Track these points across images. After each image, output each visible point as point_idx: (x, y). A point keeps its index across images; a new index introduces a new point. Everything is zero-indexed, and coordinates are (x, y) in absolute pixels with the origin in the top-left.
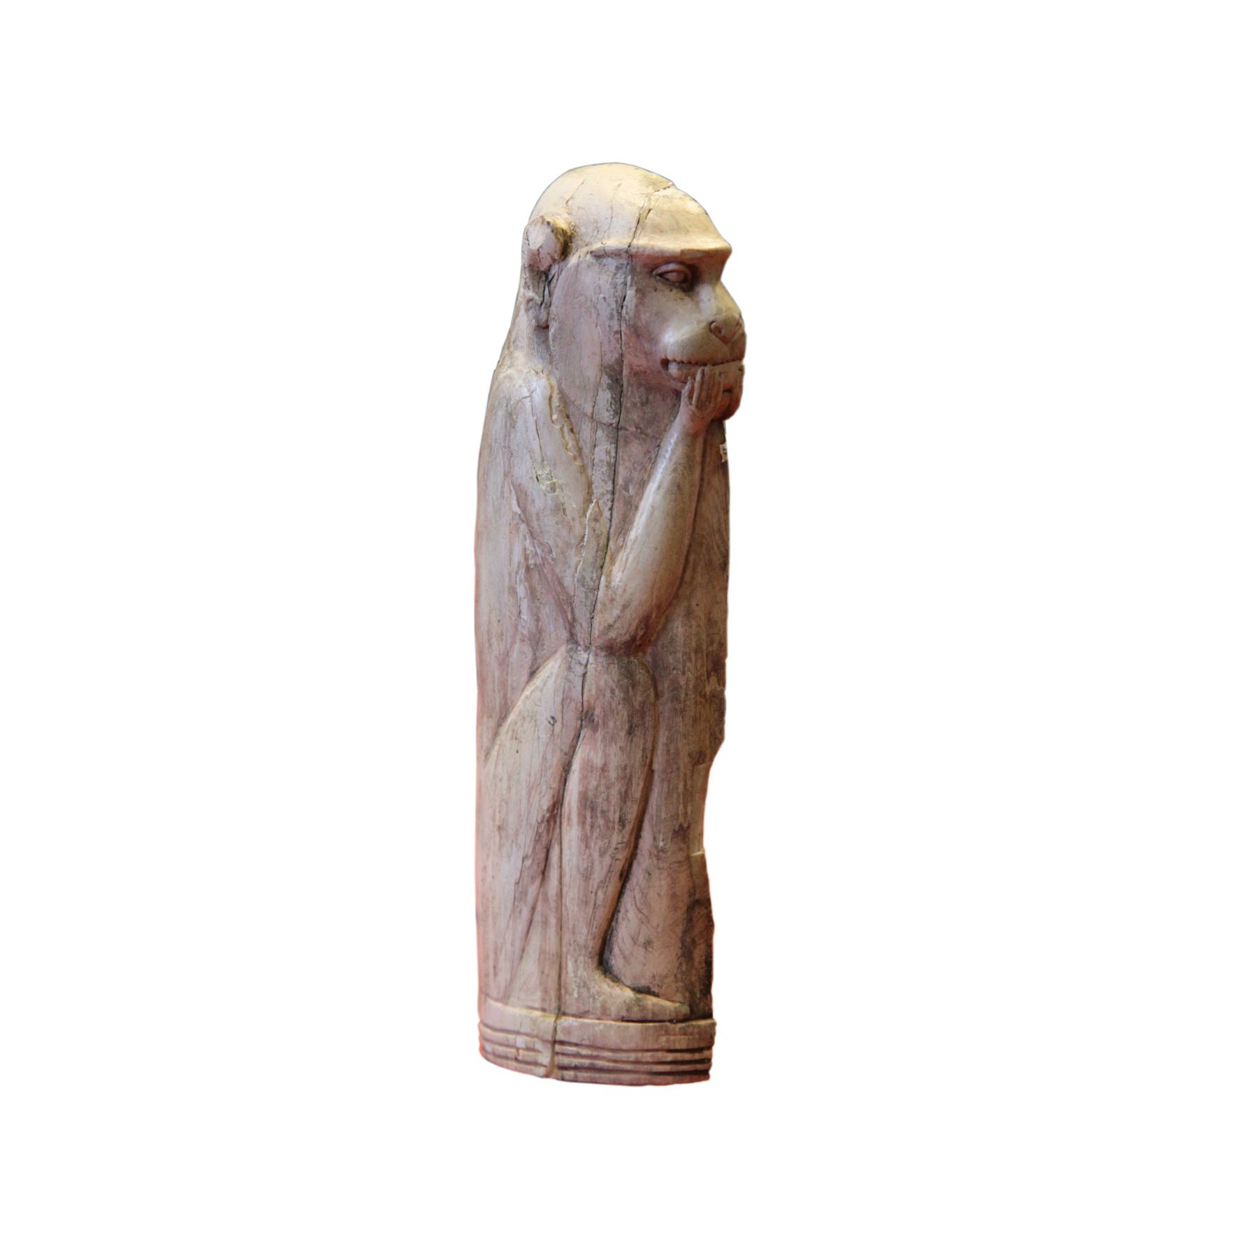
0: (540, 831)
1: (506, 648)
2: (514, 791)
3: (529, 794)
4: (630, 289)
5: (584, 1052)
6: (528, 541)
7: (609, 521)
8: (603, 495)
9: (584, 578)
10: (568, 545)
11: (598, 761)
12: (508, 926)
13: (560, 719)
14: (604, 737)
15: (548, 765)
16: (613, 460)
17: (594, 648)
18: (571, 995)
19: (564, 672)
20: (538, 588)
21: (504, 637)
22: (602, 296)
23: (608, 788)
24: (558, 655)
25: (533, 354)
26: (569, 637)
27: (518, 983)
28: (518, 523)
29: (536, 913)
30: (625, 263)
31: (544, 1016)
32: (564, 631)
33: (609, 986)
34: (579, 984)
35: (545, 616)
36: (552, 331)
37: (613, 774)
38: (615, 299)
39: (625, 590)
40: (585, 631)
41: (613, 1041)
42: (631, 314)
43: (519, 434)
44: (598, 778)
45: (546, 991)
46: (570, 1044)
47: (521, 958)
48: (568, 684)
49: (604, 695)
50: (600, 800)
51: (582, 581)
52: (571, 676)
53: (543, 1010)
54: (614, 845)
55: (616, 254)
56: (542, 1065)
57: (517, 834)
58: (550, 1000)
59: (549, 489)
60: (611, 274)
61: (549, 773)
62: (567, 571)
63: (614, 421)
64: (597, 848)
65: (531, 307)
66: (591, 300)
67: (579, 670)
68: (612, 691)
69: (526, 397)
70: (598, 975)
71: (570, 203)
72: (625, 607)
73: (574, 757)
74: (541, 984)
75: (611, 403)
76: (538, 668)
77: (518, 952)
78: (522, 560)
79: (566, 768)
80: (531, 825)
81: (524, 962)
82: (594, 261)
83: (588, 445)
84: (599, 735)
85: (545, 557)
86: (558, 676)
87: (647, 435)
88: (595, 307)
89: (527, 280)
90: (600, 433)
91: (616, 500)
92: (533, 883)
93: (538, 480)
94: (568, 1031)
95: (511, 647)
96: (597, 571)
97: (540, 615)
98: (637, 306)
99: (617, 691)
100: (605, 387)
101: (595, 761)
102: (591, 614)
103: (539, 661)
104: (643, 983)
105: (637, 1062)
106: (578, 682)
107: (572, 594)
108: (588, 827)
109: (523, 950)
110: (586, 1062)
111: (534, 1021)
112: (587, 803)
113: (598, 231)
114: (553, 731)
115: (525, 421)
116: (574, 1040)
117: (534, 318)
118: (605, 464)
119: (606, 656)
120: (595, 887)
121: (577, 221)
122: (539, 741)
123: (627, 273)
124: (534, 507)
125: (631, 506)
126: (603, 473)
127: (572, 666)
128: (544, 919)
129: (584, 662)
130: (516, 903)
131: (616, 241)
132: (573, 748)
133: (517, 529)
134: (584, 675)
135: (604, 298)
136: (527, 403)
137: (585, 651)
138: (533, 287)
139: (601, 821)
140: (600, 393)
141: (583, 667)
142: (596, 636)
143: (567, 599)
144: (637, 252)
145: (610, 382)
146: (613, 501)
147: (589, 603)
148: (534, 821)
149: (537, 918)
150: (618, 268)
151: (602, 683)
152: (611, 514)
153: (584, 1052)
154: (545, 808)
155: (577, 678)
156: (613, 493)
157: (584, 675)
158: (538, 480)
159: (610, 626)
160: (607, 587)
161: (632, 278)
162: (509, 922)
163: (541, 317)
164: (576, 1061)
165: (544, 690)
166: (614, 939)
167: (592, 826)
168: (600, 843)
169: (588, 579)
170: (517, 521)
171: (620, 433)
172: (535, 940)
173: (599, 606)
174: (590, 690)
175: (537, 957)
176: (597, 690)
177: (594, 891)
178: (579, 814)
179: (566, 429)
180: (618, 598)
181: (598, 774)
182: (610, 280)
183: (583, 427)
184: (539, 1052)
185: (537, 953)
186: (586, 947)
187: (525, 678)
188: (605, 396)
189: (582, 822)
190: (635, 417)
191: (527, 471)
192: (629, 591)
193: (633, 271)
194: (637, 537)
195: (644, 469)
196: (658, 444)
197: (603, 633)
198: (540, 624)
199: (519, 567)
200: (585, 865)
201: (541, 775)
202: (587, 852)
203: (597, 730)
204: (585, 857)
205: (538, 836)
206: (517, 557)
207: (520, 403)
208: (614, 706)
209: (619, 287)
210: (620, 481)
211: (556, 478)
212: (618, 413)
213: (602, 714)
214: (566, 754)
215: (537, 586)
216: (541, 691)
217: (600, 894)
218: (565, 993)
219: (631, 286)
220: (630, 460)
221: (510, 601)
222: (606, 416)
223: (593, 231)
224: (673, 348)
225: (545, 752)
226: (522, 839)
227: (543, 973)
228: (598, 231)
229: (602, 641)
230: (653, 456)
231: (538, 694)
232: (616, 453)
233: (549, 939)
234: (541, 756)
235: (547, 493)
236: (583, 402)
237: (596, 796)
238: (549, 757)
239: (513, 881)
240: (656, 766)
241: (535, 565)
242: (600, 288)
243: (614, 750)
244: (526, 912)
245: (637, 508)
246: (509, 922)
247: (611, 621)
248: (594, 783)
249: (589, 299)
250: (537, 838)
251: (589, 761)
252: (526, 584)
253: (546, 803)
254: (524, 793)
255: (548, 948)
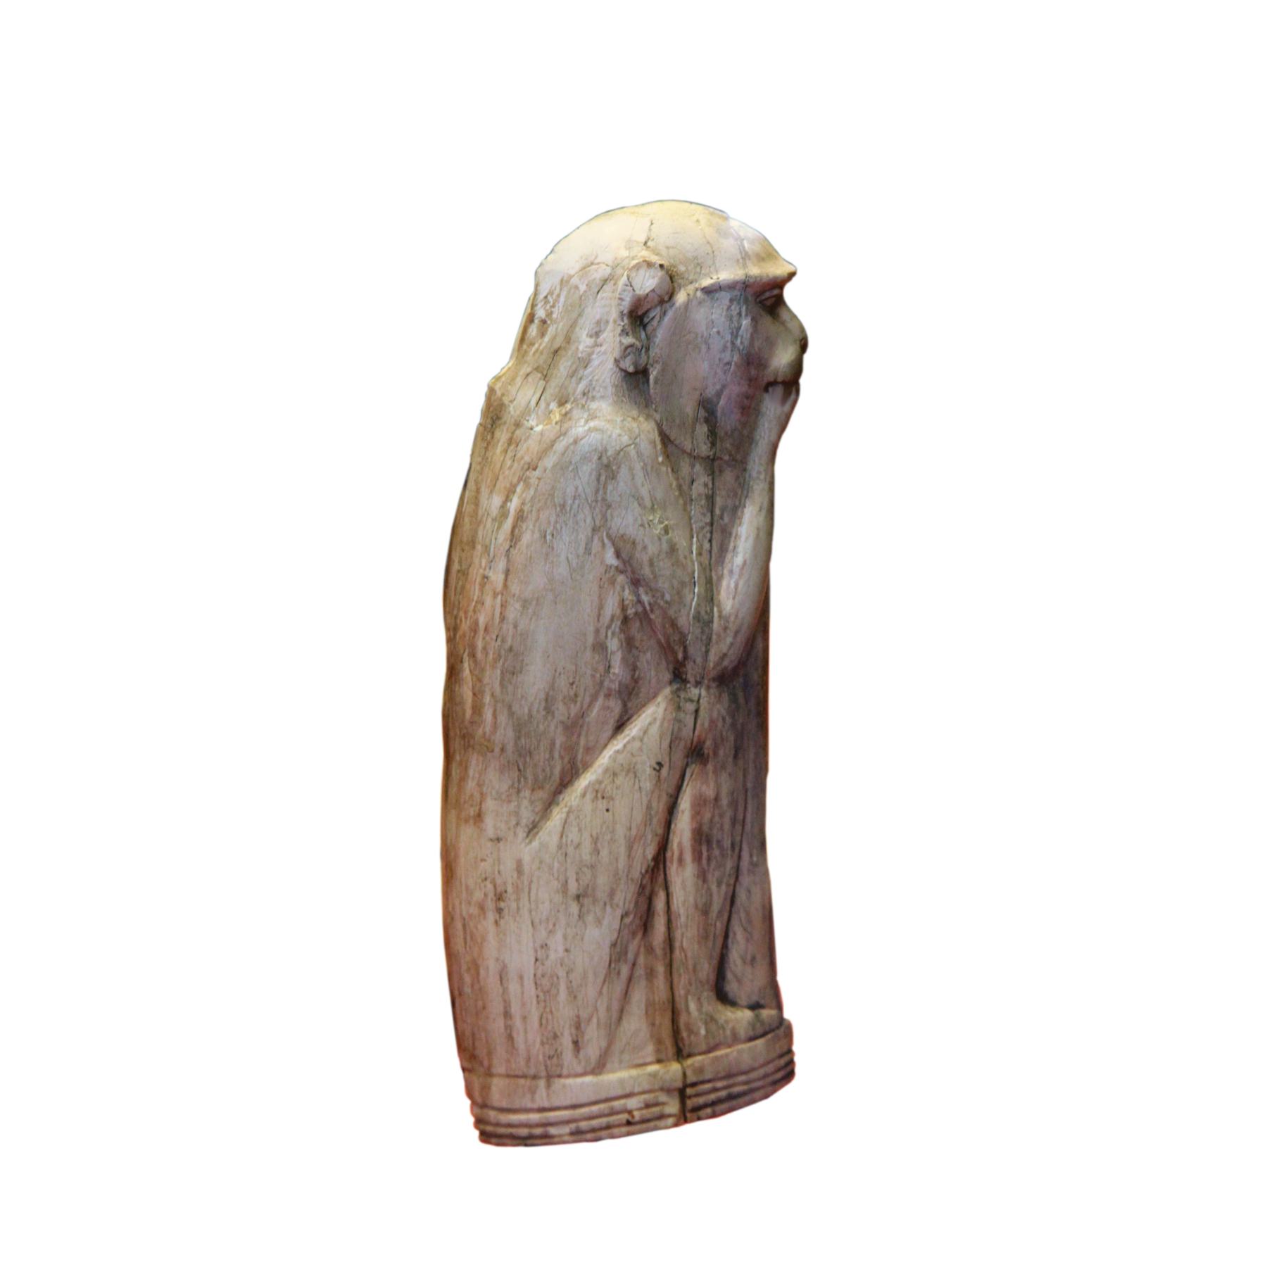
0: (644, 882)
1: (582, 708)
2: (604, 853)
3: (630, 848)
4: (745, 319)
5: (719, 1084)
6: (627, 591)
7: (708, 553)
8: (702, 528)
9: (699, 613)
10: (683, 584)
11: (710, 792)
12: (600, 993)
13: (668, 764)
14: (715, 767)
15: (652, 813)
16: (710, 492)
17: (706, 681)
18: (697, 1034)
19: (672, 713)
20: (638, 636)
21: (579, 699)
22: (715, 330)
23: (721, 816)
24: (660, 699)
25: (622, 401)
26: (673, 677)
27: (617, 1046)
28: (613, 576)
29: (637, 967)
30: (739, 294)
31: (666, 1066)
32: (667, 672)
33: (732, 1012)
34: (706, 1020)
35: (645, 664)
36: (653, 374)
37: (725, 802)
38: (730, 331)
39: (737, 616)
40: (698, 665)
41: (747, 1061)
42: (746, 343)
43: (621, 484)
44: (712, 810)
45: (659, 1042)
46: (703, 1082)
47: (620, 1019)
48: (677, 725)
49: (716, 726)
50: (715, 831)
51: (697, 617)
52: (682, 715)
53: (659, 1061)
54: (727, 873)
55: (731, 286)
56: (670, 1116)
57: (612, 894)
58: (666, 1049)
59: (663, 532)
60: (725, 308)
61: (655, 821)
62: (682, 610)
63: (711, 453)
64: (715, 879)
65: (629, 354)
66: (702, 337)
67: (691, 707)
68: (724, 719)
69: (630, 445)
70: (720, 1007)
71: (649, 244)
72: (737, 633)
73: (681, 796)
74: (652, 1036)
75: (708, 436)
76: (629, 719)
77: (615, 1015)
78: (618, 612)
79: (672, 809)
80: (632, 880)
81: (625, 1022)
82: (706, 297)
83: (687, 482)
84: (710, 767)
85: (656, 602)
86: (664, 719)
87: (736, 461)
88: (706, 343)
89: (626, 327)
90: (698, 468)
91: (714, 530)
92: (633, 938)
93: (650, 526)
94: (700, 1070)
95: (589, 706)
96: (709, 603)
97: (638, 664)
98: (752, 335)
99: (727, 718)
100: (702, 420)
101: (707, 793)
102: (706, 647)
103: (630, 712)
104: (755, 998)
105: (766, 1076)
106: (689, 720)
107: (687, 632)
108: (704, 861)
109: (622, 1011)
110: (723, 1094)
111: (654, 1075)
112: (701, 837)
113: (701, 267)
114: (659, 777)
115: (631, 469)
116: (708, 1076)
117: (633, 363)
118: (704, 497)
119: (718, 686)
120: (714, 918)
121: (672, 261)
122: (641, 792)
123: (742, 303)
124: (647, 553)
125: (727, 533)
126: (702, 506)
127: (681, 704)
128: (649, 971)
129: (696, 699)
130: (613, 965)
131: (727, 274)
132: (679, 788)
133: (612, 582)
134: (697, 711)
135: (718, 333)
136: (632, 449)
137: (696, 686)
138: (633, 333)
139: (716, 852)
140: (698, 426)
141: (695, 703)
142: (711, 669)
143: (680, 639)
144: (754, 283)
145: (707, 415)
146: (711, 533)
147: (704, 637)
148: (636, 874)
149: (640, 971)
150: (731, 301)
151: (715, 714)
152: (711, 546)
153: (719, 1084)
154: (650, 857)
155: (688, 716)
156: (712, 524)
157: (697, 711)
158: (650, 526)
159: (725, 655)
160: (720, 617)
161: (747, 308)
162: (602, 988)
163: (641, 362)
164: (713, 1097)
165: (645, 739)
166: (727, 965)
167: (709, 859)
168: (717, 874)
169: (703, 613)
170: (611, 574)
171: (716, 463)
172: (639, 997)
173: (714, 637)
174: (703, 725)
175: (644, 1012)
176: (710, 723)
177: (713, 923)
178: (694, 850)
179: (670, 470)
180: (731, 625)
181: (712, 805)
182: (724, 313)
183: (682, 464)
184: (663, 1104)
185: (643, 1006)
186: (708, 981)
187: (610, 733)
188: (702, 430)
189: (698, 857)
190: (728, 445)
191: (635, 520)
192: (740, 616)
193: (746, 301)
194: (745, 562)
195: (735, 495)
196: (542, 481)
197: (717, 664)
198: (637, 673)
199: (612, 620)
200: (704, 900)
201: (645, 825)
202: (705, 886)
203: (708, 761)
204: (704, 892)
205: (642, 887)
206: (611, 607)
207: (622, 453)
208: (724, 734)
209: (735, 319)
210: (717, 511)
211: (667, 520)
212: (713, 444)
213: (713, 746)
214: (671, 796)
215: (636, 634)
216: (641, 740)
217: (718, 924)
218: (689, 1036)
219: (746, 315)
220: (724, 489)
221: (594, 658)
222: (704, 449)
223: (695, 267)
224: (784, 370)
225: (650, 801)
226: (619, 898)
227: (653, 1024)
228: (701, 267)
229: (715, 672)
230: (742, 481)
231: (637, 744)
232: (713, 484)
233: (658, 988)
234: (644, 807)
235: (661, 536)
236: (683, 439)
237: (711, 829)
238: (654, 804)
239: (608, 943)
240: (749, 785)
241: (636, 614)
242: (713, 323)
243: (724, 777)
244: (625, 970)
245: (730, 534)
246: (602, 988)
247: (725, 650)
248: (708, 816)
249: (700, 336)
250: (640, 891)
251: (701, 796)
252: (622, 636)
253: (650, 852)
254: (622, 850)
255: (657, 999)
